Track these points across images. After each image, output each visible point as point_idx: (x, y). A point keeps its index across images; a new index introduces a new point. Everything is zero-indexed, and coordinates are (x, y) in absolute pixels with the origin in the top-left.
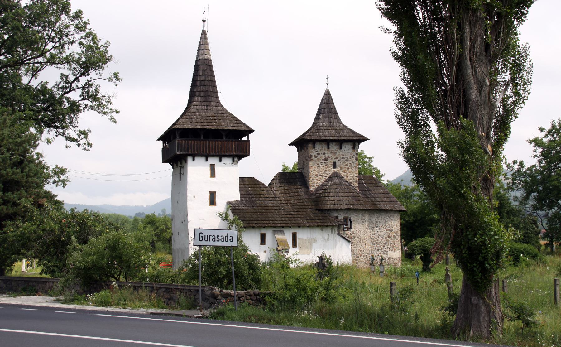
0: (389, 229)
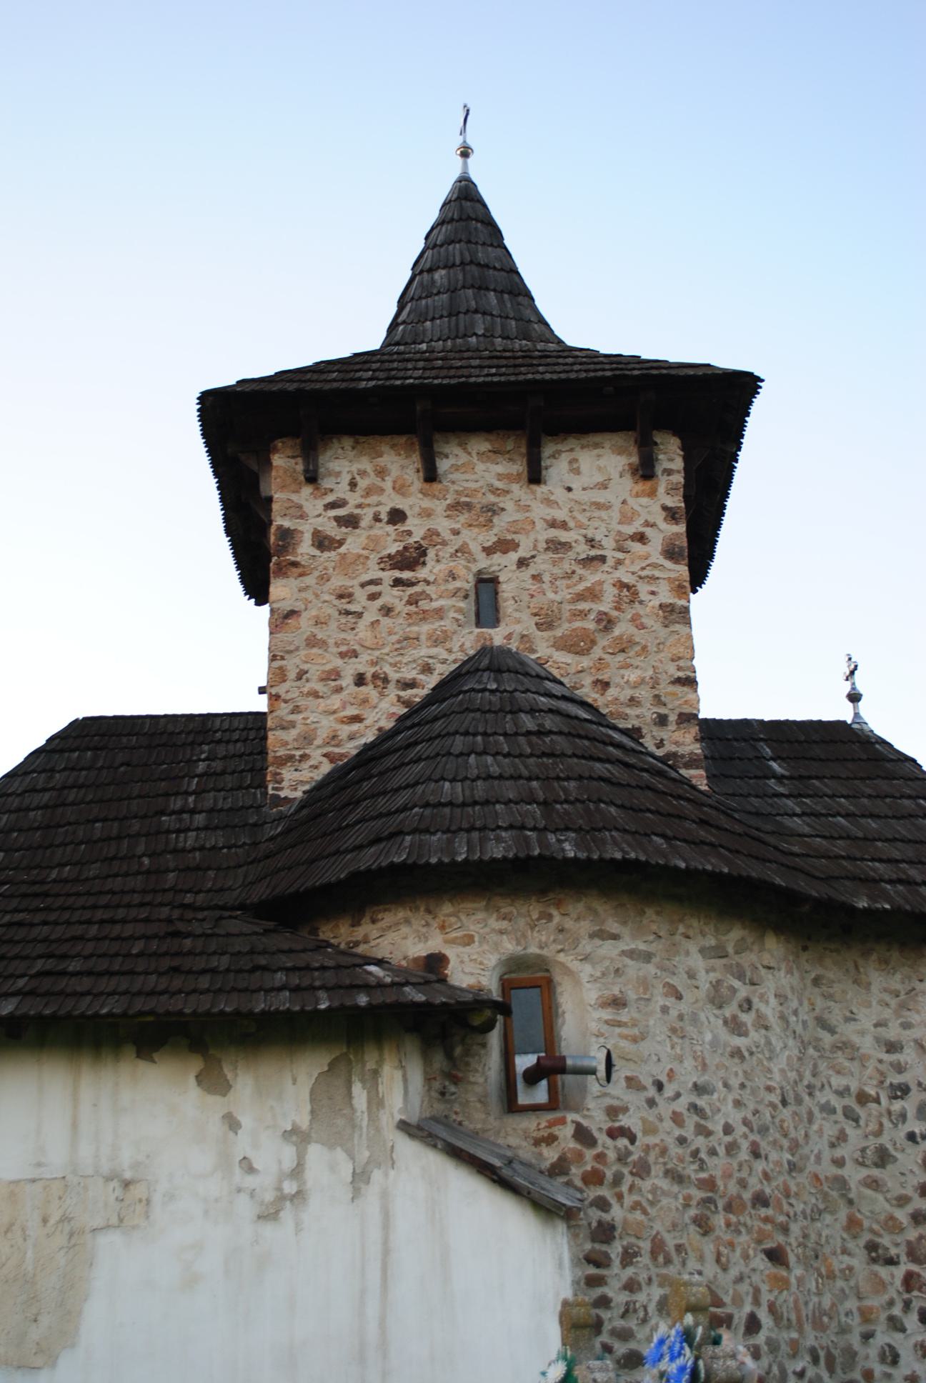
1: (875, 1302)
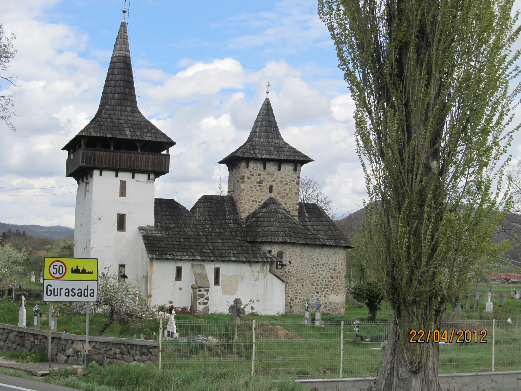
0: (332, 268)
1: (311, 290)
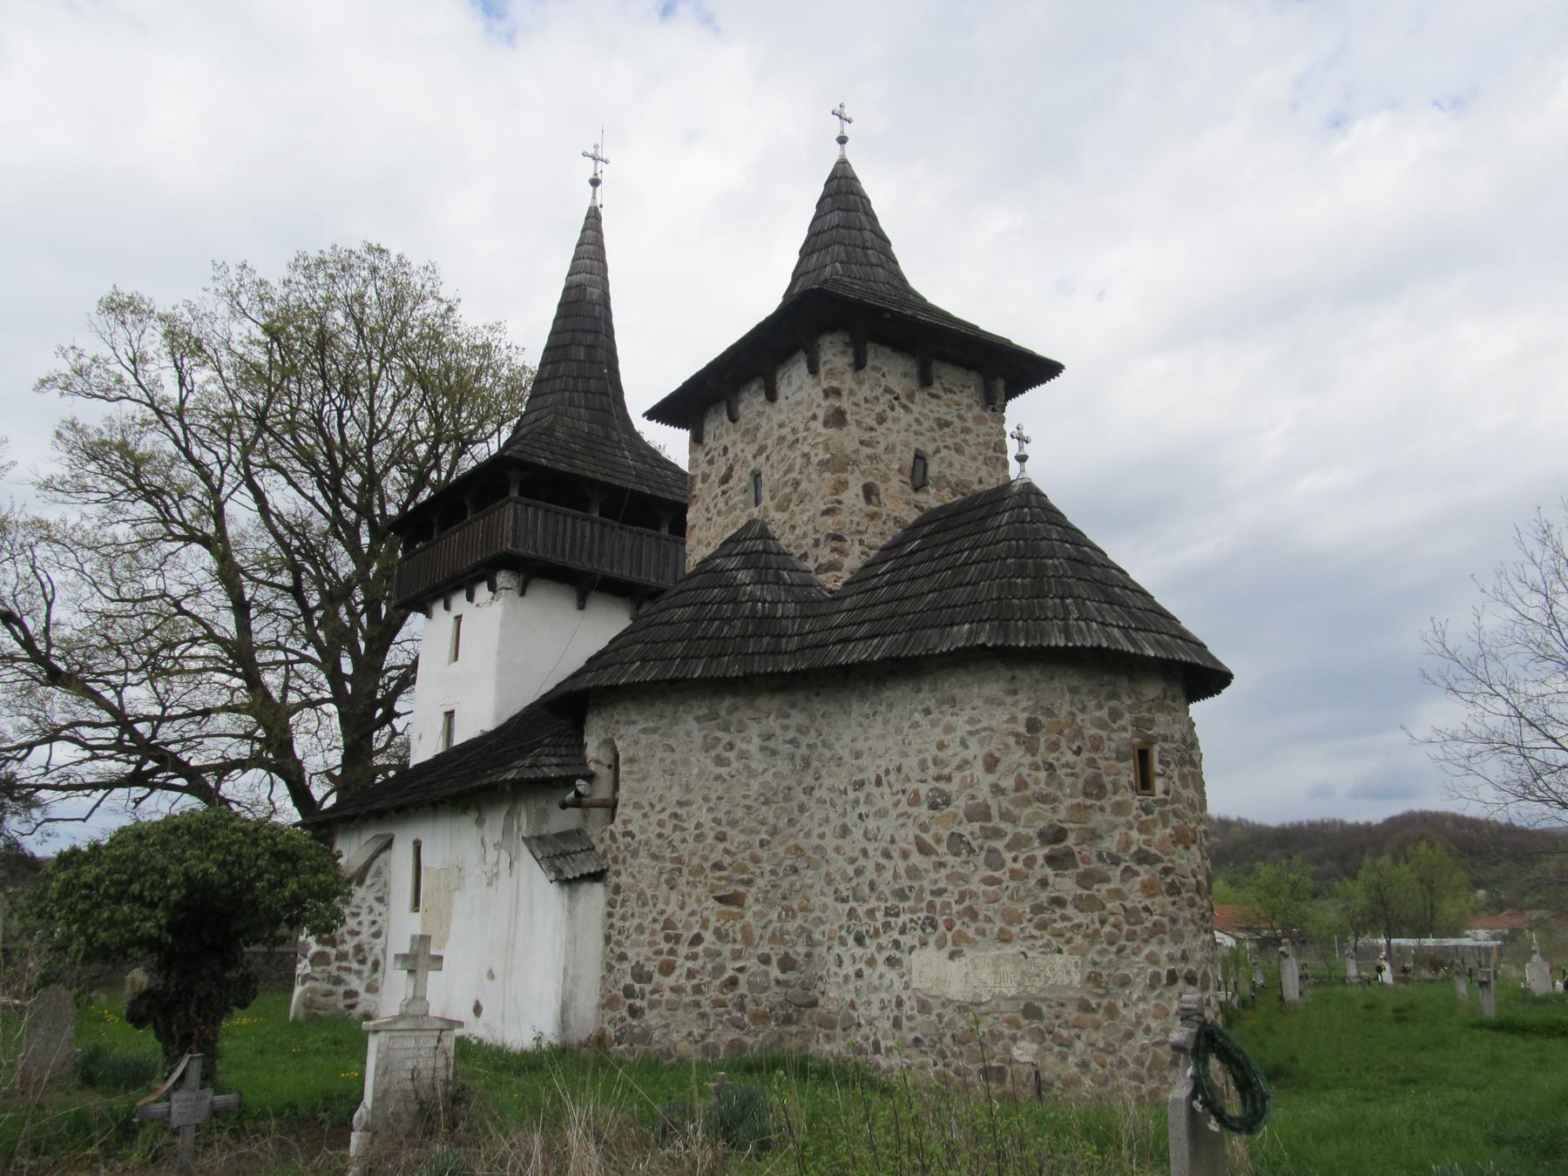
0: (924, 790)
